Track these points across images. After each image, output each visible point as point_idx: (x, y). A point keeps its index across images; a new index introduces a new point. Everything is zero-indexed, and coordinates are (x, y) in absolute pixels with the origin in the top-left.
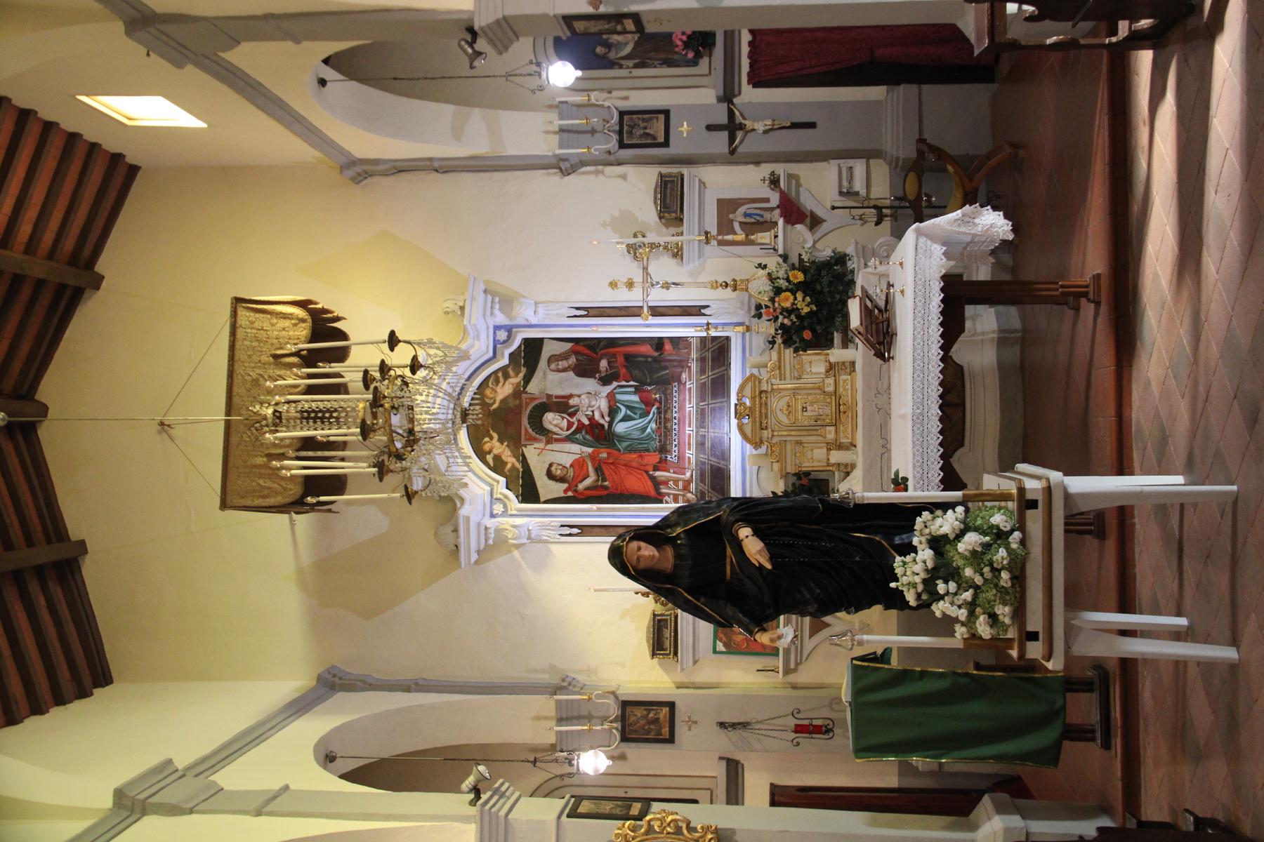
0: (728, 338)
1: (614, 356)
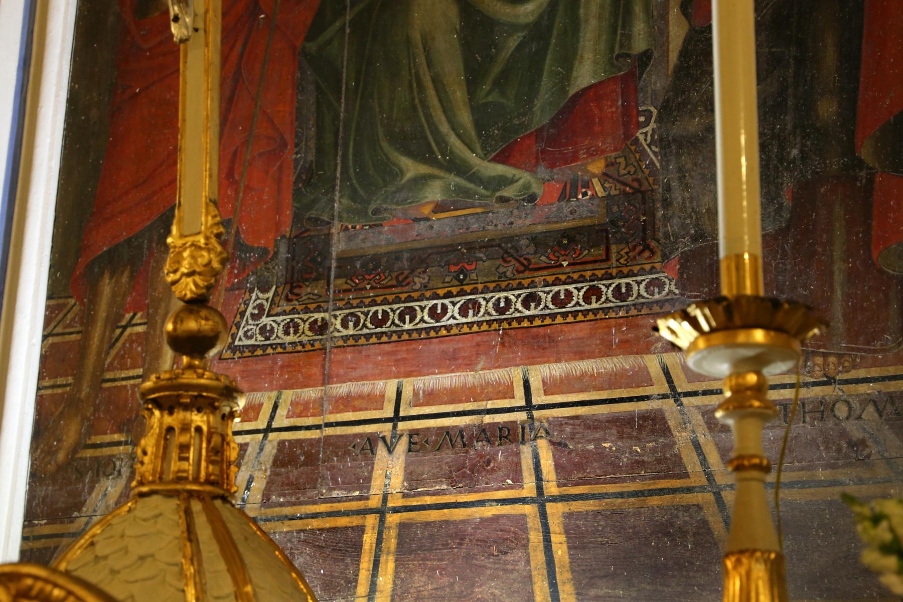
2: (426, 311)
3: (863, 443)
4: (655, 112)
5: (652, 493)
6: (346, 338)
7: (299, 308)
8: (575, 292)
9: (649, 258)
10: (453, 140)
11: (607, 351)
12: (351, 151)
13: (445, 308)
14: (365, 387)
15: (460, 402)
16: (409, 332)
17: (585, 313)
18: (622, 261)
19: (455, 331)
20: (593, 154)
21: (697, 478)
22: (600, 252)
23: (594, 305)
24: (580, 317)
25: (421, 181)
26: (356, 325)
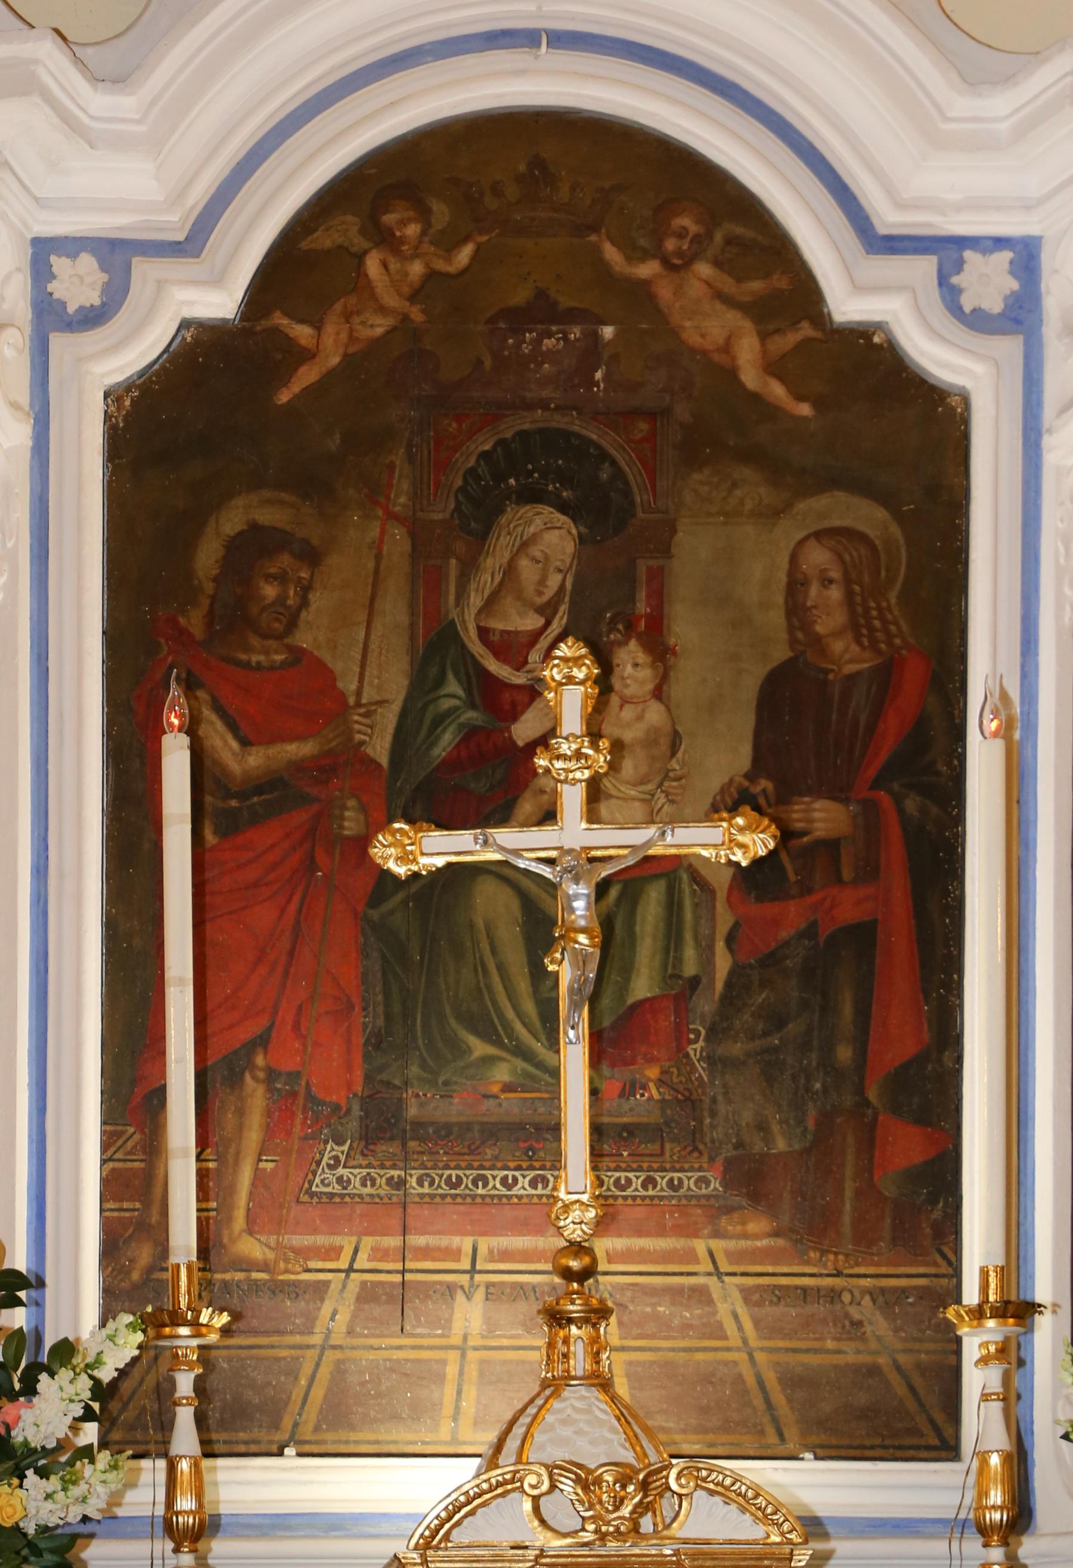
0: (945, 1446)
1: (870, 871)
2: (498, 1179)
3: (860, 1324)
4: (703, 1032)
5: (698, 1350)
6: (422, 1196)
7: (375, 1163)
8: (634, 1179)
9: (698, 1158)
10: (519, 1027)
11: (661, 1231)
12: (419, 1021)
13: (515, 1180)
14: (444, 1241)
15: (532, 1262)
16: (483, 1197)
17: (643, 1198)
18: (675, 1158)
19: (525, 1200)
20: (651, 1060)
21: (734, 1340)
22: (654, 1147)
23: (651, 1193)
24: (638, 1201)
25: (488, 1061)
26: (432, 1184)
